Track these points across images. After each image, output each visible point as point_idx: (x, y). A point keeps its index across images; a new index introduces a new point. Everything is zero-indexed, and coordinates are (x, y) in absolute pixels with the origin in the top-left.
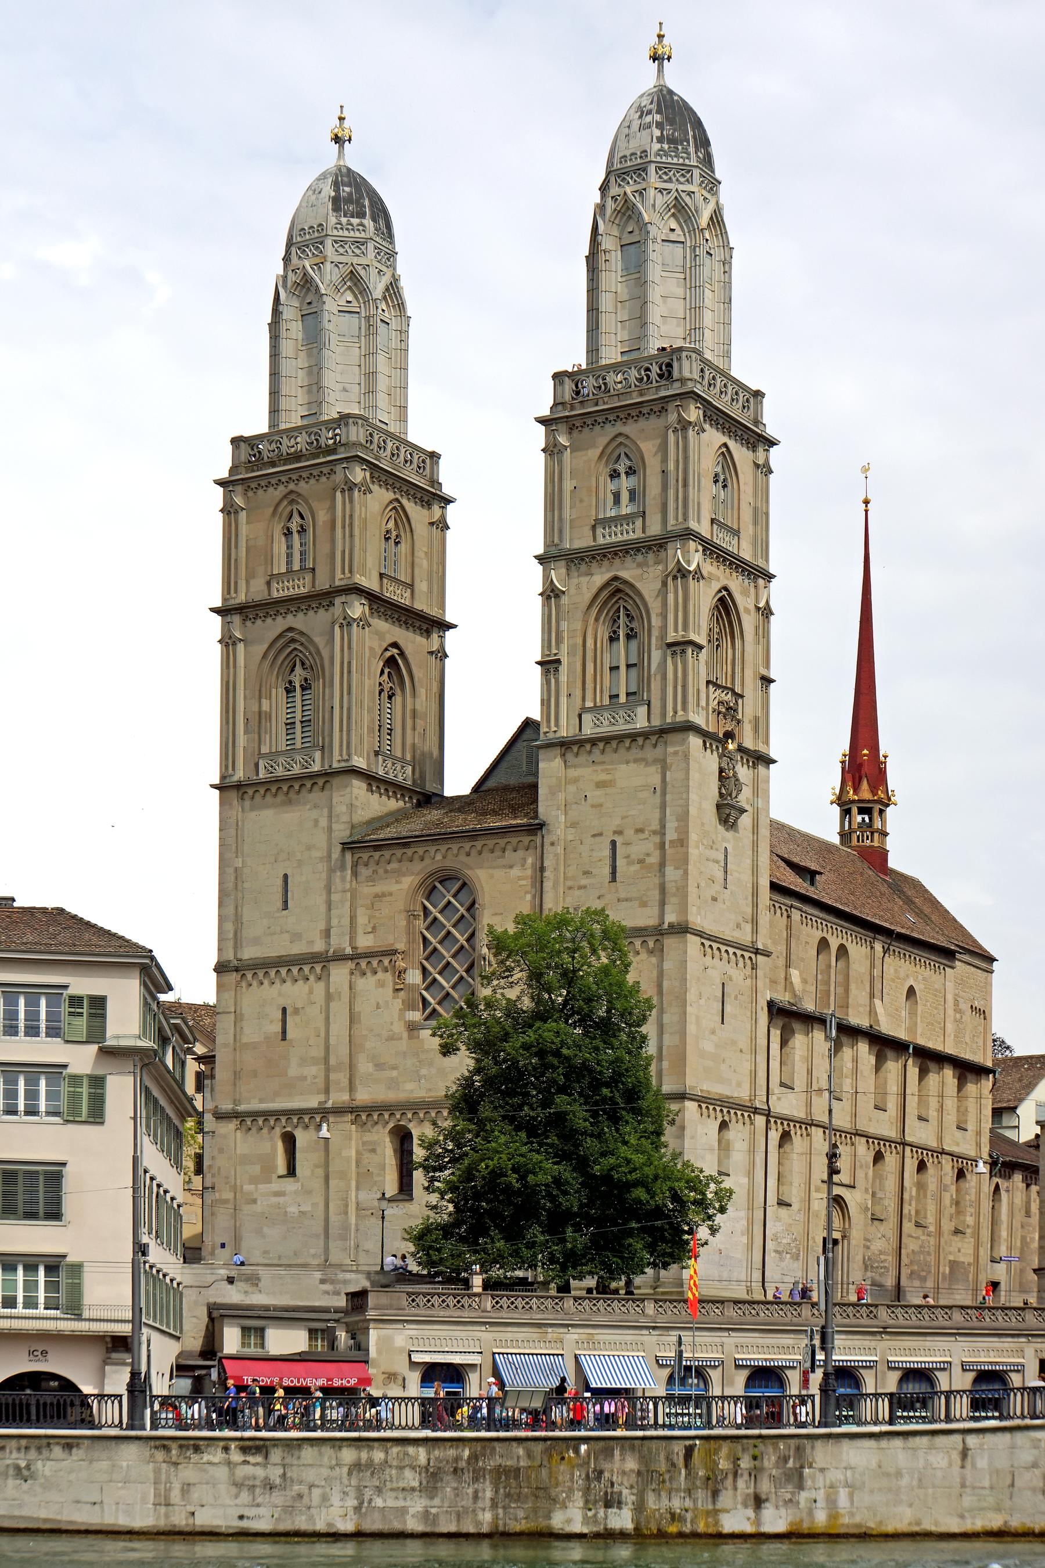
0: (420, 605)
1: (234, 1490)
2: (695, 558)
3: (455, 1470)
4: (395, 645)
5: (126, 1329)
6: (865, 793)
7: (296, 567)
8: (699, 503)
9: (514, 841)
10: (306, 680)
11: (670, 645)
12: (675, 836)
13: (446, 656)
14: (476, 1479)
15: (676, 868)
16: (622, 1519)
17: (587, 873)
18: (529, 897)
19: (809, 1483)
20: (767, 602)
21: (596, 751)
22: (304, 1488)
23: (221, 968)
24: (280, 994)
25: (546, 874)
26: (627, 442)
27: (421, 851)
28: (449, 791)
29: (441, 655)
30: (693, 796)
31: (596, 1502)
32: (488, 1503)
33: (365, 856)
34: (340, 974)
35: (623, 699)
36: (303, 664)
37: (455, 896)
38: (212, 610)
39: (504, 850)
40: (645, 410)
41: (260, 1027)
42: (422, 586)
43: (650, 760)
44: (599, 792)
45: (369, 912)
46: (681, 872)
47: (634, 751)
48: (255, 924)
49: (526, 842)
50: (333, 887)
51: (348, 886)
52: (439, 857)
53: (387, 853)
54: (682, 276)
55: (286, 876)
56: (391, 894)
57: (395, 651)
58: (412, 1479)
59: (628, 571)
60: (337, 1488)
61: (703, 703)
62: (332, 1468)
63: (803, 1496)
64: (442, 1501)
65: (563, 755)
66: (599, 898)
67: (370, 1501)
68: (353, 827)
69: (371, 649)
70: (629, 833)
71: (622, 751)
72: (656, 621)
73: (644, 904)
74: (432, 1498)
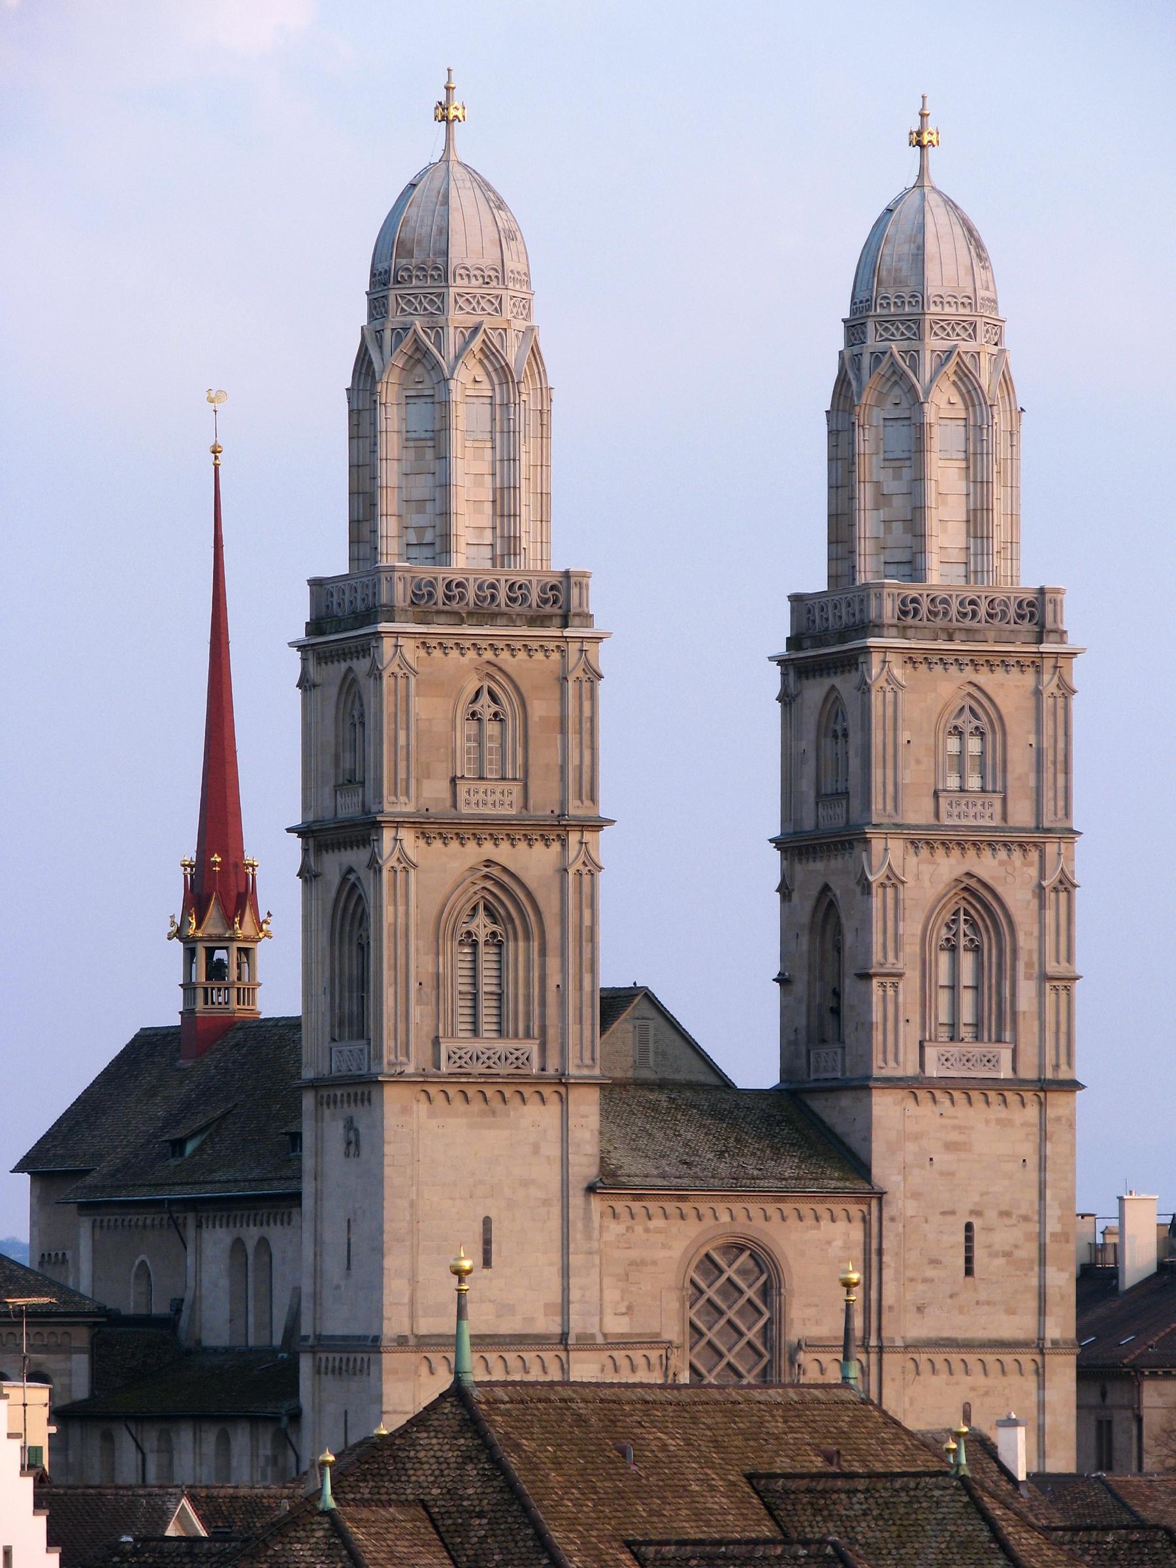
6: (213, 925)
9: (837, 1209)
15: (1061, 1269)
25: (885, 1259)
27: (704, 1208)
33: (620, 1206)
35: (966, 1032)
36: (486, 908)
50: (572, 1246)
53: (653, 1206)
55: (487, 1222)
56: (654, 1263)
59: (987, 866)
66: (951, 1296)
70: (991, 1215)
72: (1026, 942)
73: (1011, 1312)
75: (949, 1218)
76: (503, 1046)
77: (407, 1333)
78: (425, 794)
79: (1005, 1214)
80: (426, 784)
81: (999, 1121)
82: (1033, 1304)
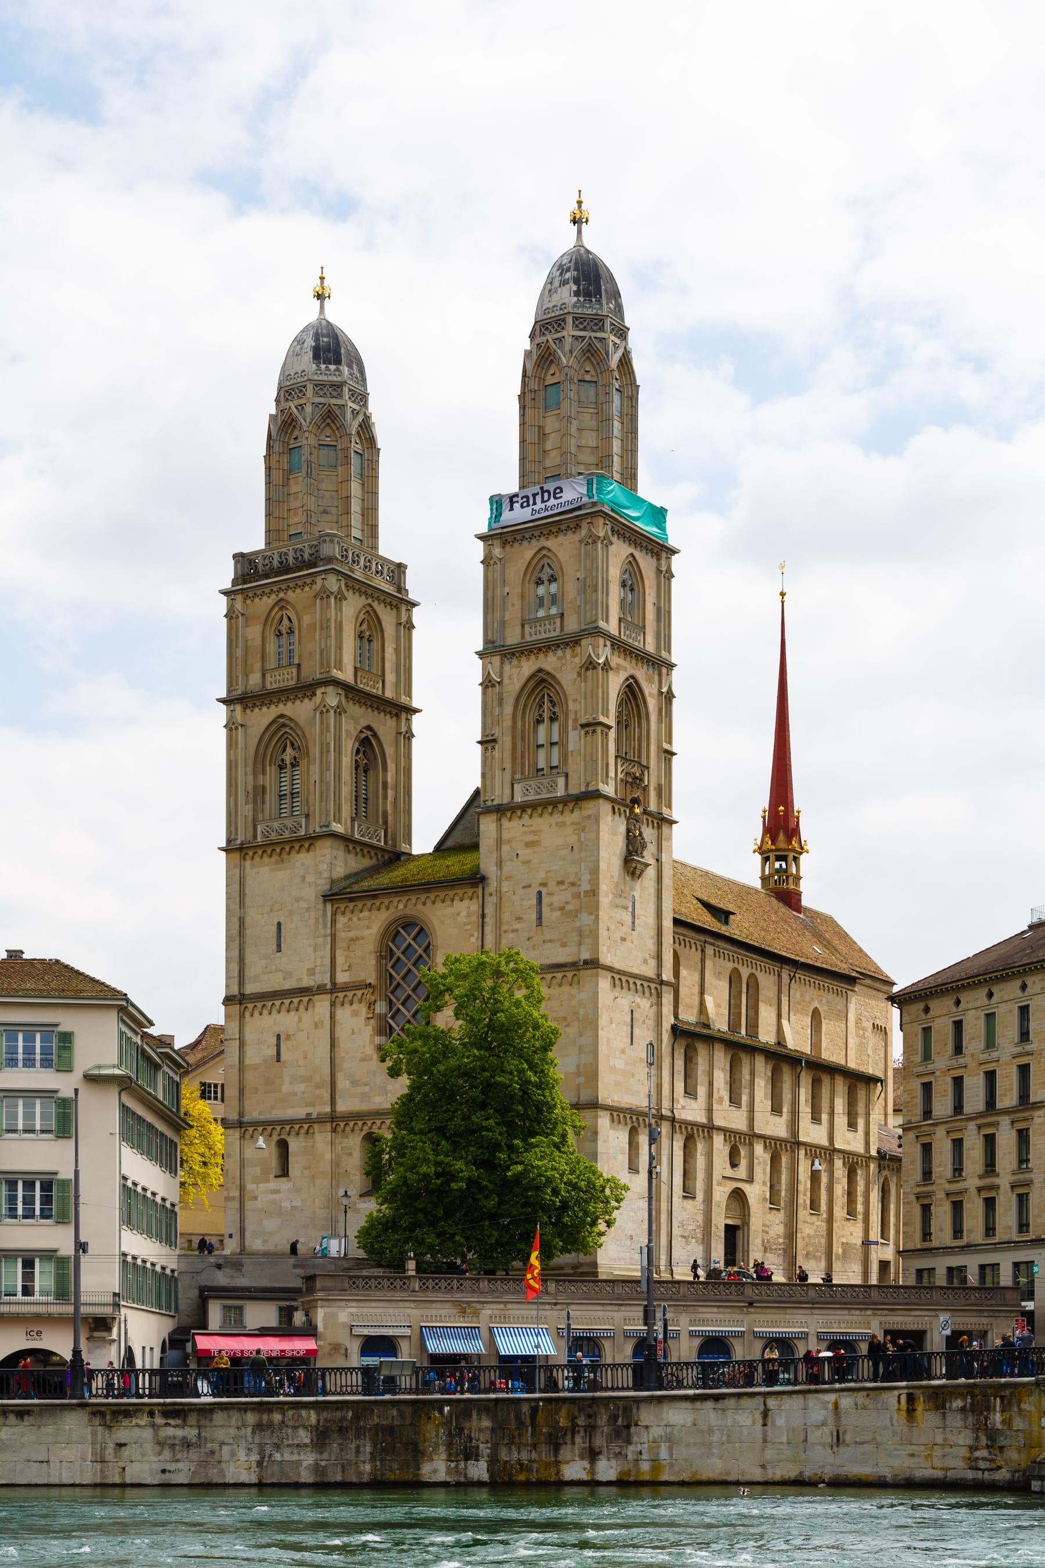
0: (389, 694)
1: (158, 1448)
2: (604, 653)
3: (341, 1428)
4: (369, 728)
5: (108, 1310)
7: (284, 663)
8: (607, 606)
9: (460, 892)
10: (295, 758)
11: (583, 726)
12: (588, 888)
13: (413, 736)
14: (358, 1437)
15: (590, 914)
16: (479, 1470)
17: (518, 919)
18: (473, 940)
19: (635, 1439)
20: (670, 688)
21: (526, 817)
22: (216, 1446)
23: (228, 1001)
24: (275, 1023)
25: (486, 920)
26: (549, 554)
28: (415, 851)
29: (409, 736)
30: (603, 854)
31: (457, 1455)
32: (368, 1456)
33: (342, 906)
34: (322, 1005)
36: (293, 745)
37: (414, 939)
38: (219, 700)
39: (452, 900)
40: (563, 528)
41: (258, 1053)
42: (390, 677)
43: (568, 823)
44: (528, 851)
45: (345, 953)
46: (593, 917)
47: (555, 816)
48: (255, 964)
49: (470, 894)
51: (329, 931)
52: (401, 906)
53: (360, 904)
54: (595, 411)
56: (363, 938)
57: (369, 733)
58: (304, 1436)
60: (243, 1444)
61: (612, 774)
62: (238, 1428)
63: (631, 1451)
64: (330, 1455)
65: (499, 820)
67: (270, 1456)
68: (332, 882)
69: (347, 731)
70: (552, 884)
71: (546, 816)
73: (564, 945)
74: (321, 1453)
75: (528, 890)
76: (288, 822)
77: (237, 993)
78: (251, 683)
79: (561, 883)
80: (251, 676)
81: (557, 824)
82: (576, 939)
